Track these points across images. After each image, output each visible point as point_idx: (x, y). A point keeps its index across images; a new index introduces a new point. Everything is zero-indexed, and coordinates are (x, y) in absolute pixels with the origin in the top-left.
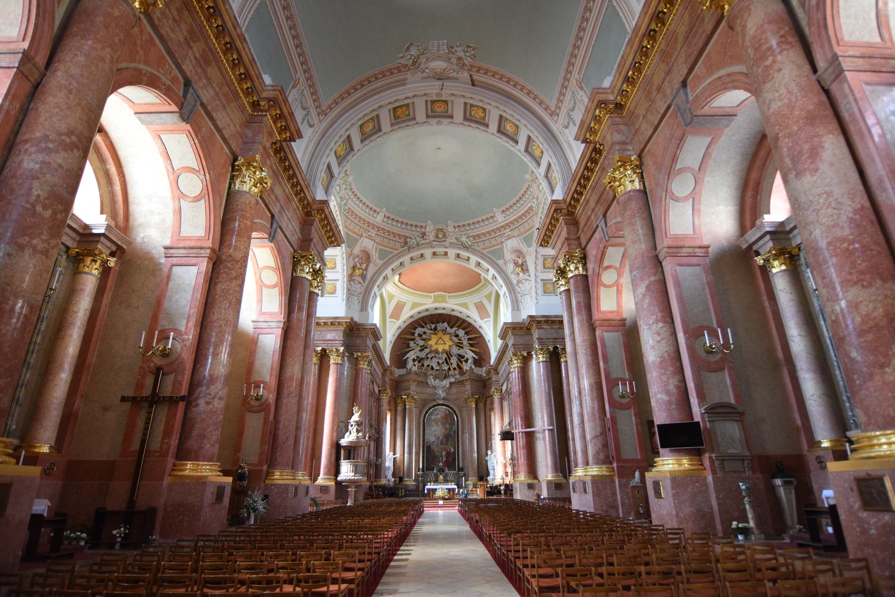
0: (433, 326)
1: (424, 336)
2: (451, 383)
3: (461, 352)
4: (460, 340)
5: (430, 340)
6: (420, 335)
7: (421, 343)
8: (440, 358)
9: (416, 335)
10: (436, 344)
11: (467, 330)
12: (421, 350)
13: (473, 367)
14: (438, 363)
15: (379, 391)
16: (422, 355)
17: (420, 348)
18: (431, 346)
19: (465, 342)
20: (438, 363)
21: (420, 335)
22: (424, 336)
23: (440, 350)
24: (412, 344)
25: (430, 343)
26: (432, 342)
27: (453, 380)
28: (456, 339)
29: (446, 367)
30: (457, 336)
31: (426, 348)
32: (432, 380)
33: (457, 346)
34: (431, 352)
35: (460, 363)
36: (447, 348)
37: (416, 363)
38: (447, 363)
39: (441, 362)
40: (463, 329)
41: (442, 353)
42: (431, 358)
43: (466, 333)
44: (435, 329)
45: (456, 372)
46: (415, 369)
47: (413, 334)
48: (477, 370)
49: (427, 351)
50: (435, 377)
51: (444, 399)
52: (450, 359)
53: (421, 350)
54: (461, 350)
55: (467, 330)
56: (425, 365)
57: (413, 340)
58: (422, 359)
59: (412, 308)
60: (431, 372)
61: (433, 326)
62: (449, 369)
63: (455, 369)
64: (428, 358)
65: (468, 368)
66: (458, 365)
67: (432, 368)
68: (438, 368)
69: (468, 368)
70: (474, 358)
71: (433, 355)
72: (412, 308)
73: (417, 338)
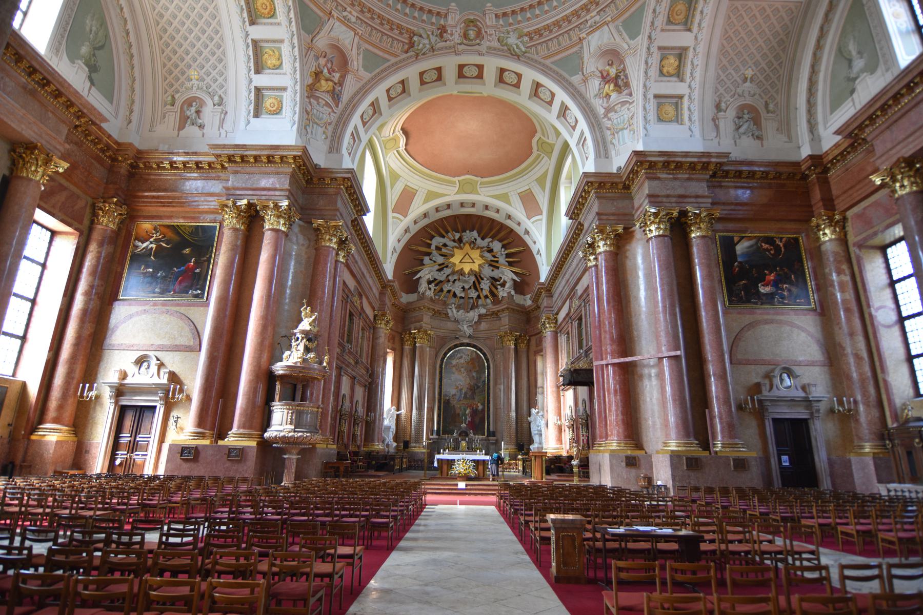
0: (457, 236)
1: (444, 250)
3: (496, 274)
4: (494, 257)
5: (452, 256)
6: (438, 248)
7: (440, 260)
8: (465, 282)
9: (433, 247)
10: (460, 262)
11: (505, 242)
12: (439, 270)
13: (513, 292)
14: (463, 288)
16: (441, 276)
17: (437, 267)
18: (454, 264)
19: (502, 260)
20: (463, 288)
21: (438, 248)
22: (444, 250)
23: (467, 270)
24: (426, 260)
25: (452, 260)
26: (456, 260)
27: (483, 311)
28: (489, 256)
29: (474, 294)
30: (490, 251)
31: (447, 267)
32: (455, 311)
33: (491, 265)
34: (453, 273)
35: (493, 289)
36: (476, 267)
37: (432, 286)
39: (467, 287)
40: (500, 241)
41: (469, 274)
43: (504, 246)
45: (488, 301)
46: (430, 293)
47: (429, 245)
48: (518, 299)
49: (447, 271)
50: (459, 308)
51: (470, 337)
52: (479, 283)
53: (439, 270)
54: (496, 271)
55: (505, 242)
56: (445, 290)
57: (429, 254)
58: (441, 282)
59: (426, 201)
60: (453, 300)
61: (457, 236)
62: (479, 297)
63: (486, 297)
64: (449, 281)
65: (505, 295)
66: (491, 291)
67: (455, 295)
68: (463, 295)
69: (505, 295)
70: (514, 280)
71: (456, 277)
72: (426, 201)
73: (435, 252)
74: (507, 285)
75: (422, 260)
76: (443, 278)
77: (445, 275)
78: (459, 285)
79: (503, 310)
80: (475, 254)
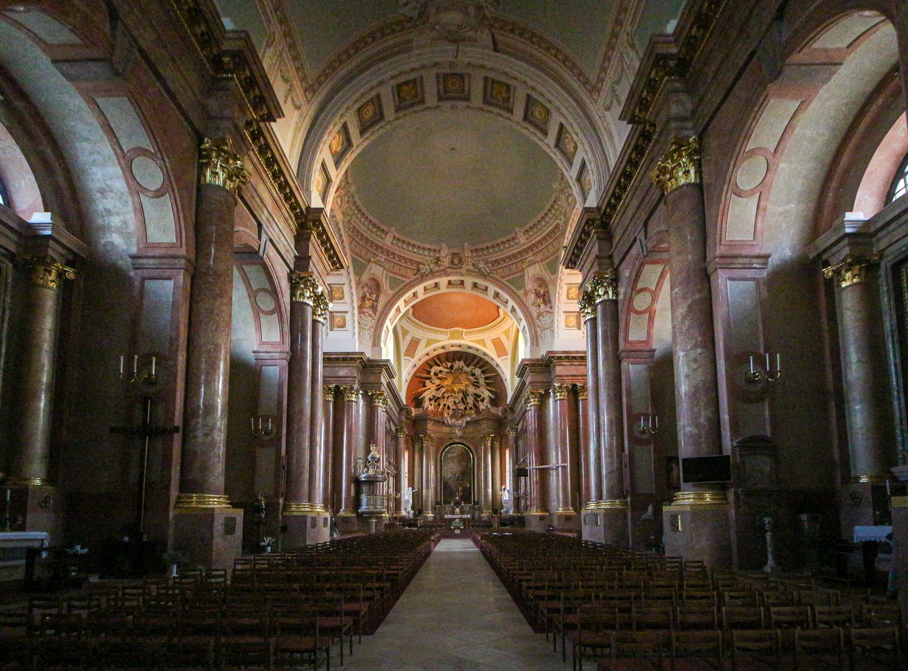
0: (449, 364)
1: (440, 375)
2: (467, 423)
3: (478, 391)
7: (437, 382)
8: (456, 397)
9: (432, 374)
12: (438, 389)
13: (489, 406)
14: (455, 402)
15: (397, 429)
17: (436, 388)
19: (482, 381)
20: (455, 402)
21: (436, 374)
24: (428, 382)
27: (469, 419)
28: (471, 377)
29: (462, 407)
30: (473, 375)
33: (473, 385)
34: (447, 391)
36: (462, 387)
37: (433, 402)
38: (463, 402)
39: (457, 401)
40: (480, 368)
42: (448, 398)
43: (483, 372)
44: (452, 367)
47: (429, 373)
48: (493, 410)
49: (443, 390)
50: (453, 416)
51: (460, 437)
52: (466, 398)
53: (438, 389)
54: (478, 389)
57: (429, 379)
58: (439, 398)
61: (449, 364)
62: (466, 409)
63: (471, 408)
66: (474, 405)
67: (449, 408)
68: (455, 408)
73: (433, 377)
74: (486, 401)
75: (424, 383)
76: (440, 395)
77: (441, 394)
78: (451, 399)
79: (482, 420)
80: (463, 377)
